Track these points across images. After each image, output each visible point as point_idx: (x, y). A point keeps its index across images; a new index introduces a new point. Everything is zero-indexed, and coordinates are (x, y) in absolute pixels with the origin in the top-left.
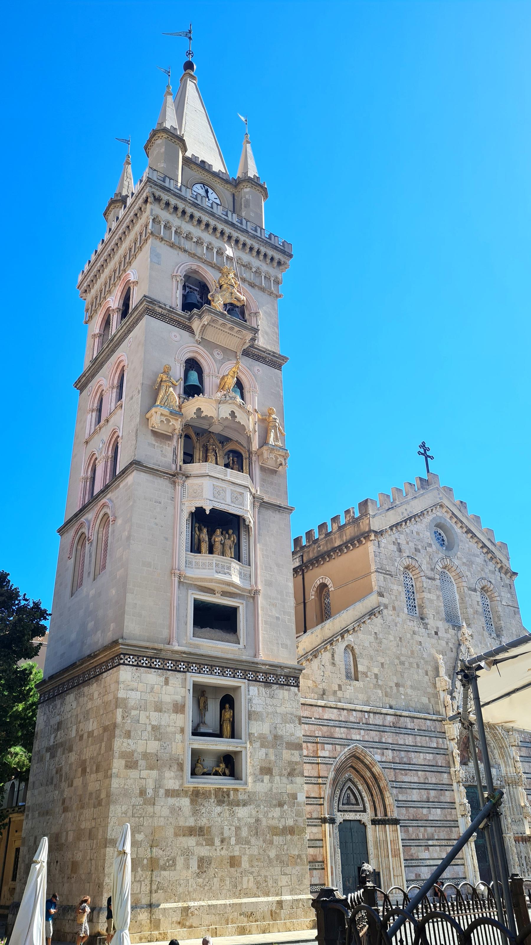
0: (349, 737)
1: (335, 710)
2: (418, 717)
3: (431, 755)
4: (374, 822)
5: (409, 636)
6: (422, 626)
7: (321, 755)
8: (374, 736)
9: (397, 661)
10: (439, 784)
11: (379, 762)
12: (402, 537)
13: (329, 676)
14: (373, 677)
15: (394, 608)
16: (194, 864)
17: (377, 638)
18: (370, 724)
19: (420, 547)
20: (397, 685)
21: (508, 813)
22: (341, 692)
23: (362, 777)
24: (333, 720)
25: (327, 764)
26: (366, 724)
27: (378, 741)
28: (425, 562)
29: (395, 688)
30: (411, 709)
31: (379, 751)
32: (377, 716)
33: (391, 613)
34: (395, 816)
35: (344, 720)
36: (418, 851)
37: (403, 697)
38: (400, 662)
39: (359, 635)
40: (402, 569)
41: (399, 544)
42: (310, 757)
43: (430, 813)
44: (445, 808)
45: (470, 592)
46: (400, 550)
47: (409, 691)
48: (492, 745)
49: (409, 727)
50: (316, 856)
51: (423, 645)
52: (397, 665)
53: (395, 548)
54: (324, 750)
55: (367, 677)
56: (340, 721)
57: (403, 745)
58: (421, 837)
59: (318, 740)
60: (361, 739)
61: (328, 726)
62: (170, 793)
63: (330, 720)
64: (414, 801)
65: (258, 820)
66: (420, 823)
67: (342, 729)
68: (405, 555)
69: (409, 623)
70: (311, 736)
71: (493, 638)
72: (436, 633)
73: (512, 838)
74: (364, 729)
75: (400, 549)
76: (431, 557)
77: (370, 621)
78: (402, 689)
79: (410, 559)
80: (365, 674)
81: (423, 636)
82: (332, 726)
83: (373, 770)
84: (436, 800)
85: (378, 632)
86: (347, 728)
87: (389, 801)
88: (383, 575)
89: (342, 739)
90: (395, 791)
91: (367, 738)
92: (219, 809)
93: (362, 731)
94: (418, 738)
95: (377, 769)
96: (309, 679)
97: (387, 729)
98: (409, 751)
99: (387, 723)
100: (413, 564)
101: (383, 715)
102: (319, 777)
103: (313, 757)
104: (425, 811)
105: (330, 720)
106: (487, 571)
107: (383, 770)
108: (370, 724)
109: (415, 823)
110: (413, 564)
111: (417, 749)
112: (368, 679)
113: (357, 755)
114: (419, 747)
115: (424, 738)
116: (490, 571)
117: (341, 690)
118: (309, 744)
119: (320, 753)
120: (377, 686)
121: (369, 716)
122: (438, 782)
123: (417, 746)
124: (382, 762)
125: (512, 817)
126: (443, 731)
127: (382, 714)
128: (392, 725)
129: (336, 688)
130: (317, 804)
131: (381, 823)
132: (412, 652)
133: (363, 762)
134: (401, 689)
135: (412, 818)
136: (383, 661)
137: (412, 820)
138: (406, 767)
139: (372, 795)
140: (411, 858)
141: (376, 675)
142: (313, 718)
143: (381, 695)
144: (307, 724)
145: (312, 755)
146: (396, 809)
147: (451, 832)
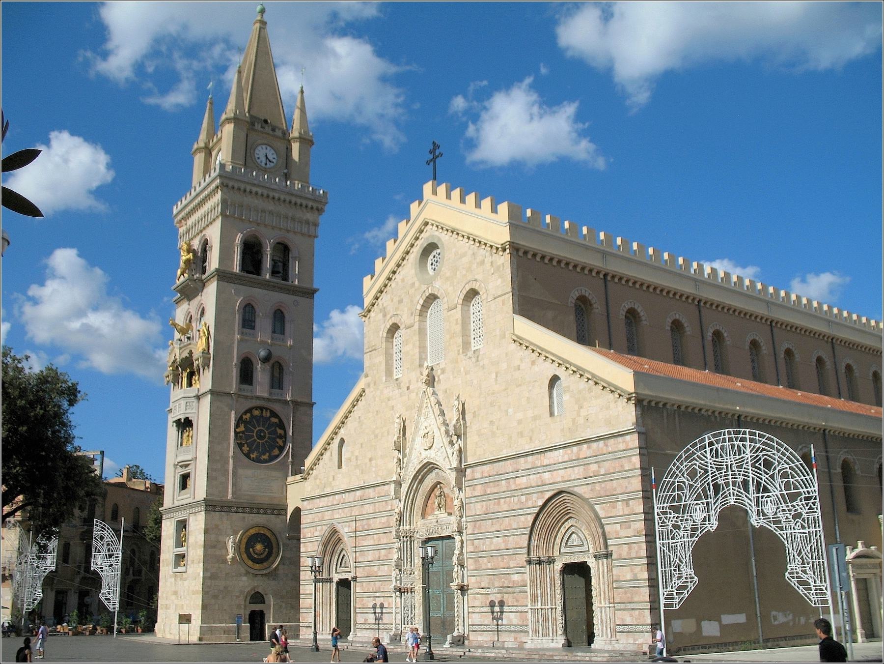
14: (355, 459)
15: (375, 384)
16: (174, 606)
28: (406, 309)
36: (368, 602)
43: (379, 569)
53: (381, 314)
58: (371, 590)
62: (171, 577)
65: (189, 587)
72: (408, 388)
84: (385, 558)
92: (180, 582)
104: (376, 568)
109: (368, 579)
111: (375, 515)
120: (357, 466)
134: (374, 462)
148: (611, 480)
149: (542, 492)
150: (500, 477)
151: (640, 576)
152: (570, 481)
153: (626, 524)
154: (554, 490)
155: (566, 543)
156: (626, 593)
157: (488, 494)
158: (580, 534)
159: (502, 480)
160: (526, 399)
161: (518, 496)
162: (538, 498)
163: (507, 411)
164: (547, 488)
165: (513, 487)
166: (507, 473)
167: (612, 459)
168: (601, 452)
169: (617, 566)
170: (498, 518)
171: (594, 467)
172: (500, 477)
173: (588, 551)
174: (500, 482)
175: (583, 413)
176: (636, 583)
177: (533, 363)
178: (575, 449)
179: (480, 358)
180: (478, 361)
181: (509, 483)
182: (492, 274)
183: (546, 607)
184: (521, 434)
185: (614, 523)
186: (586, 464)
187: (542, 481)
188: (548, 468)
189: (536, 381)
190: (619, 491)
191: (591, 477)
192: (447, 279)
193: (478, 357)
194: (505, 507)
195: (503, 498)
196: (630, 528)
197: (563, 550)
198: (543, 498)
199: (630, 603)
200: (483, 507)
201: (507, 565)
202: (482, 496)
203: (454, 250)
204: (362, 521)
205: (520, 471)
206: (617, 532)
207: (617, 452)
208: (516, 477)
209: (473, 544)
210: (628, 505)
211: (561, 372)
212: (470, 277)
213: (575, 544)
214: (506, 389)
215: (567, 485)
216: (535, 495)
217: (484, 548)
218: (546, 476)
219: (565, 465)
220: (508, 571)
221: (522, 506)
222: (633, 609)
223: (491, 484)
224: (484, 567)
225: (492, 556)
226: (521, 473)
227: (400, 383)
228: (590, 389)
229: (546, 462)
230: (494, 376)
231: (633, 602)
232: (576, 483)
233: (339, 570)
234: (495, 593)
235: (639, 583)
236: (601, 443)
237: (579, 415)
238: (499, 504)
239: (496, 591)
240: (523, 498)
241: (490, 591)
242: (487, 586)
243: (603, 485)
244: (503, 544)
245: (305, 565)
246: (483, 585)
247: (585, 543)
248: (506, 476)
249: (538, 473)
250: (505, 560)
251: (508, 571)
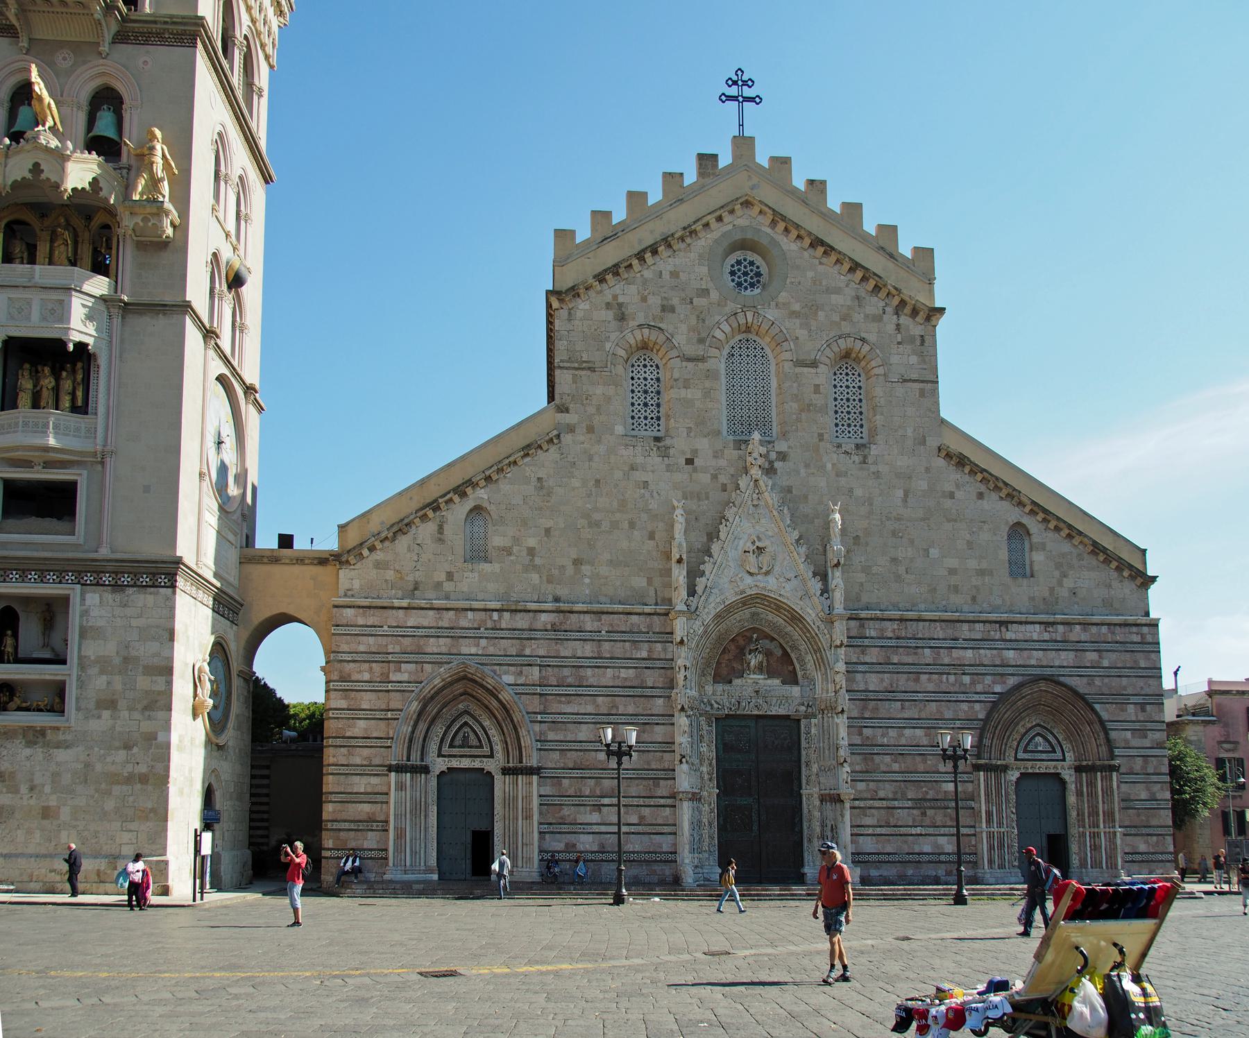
0: (455, 651)
1: (431, 613)
2: (610, 610)
3: (631, 671)
4: (506, 771)
5: (618, 474)
6: (654, 453)
7: (394, 679)
8: (511, 647)
9: (582, 522)
10: (642, 715)
11: (509, 685)
12: (633, 289)
13: (429, 560)
14: (524, 553)
15: (590, 429)
17: (542, 488)
18: (502, 630)
19: (675, 301)
20: (577, 562)
21: (813, 756)
22: (451, 583)
23: (487, 707)
24: (425, 628)
25: (404, 691)
26: (492, 629)
27: (515, 654)
28: (683, 328)
29: (570, 570)
30: (602, 599)
31: (512, 669)
32: (519, 615)
33: (582, 438)
34: (534, 762)
35: (447, 625)
37: (587, 581)
38: (590, 525)
39: (502, 486)
40: (622, 353)
41: (620, 305)
42: (376, 682)
44: (648, 751)
45: (798, 370)
46: (622, 318)
47: (604, 570)
48: (802, 648)
49: (589, 629)
50: (374, 814)
51: (651, 487)
52: (583, 527)
53: (609, 315)
54: (400, 671)
55: (510, 554)
56: (438, 628)
57: (571, 658)
58: (587, 793)
59: (390, 657)
60: (480, 653)
61: (414, 636)
63: (418, 628)
64: (581, 742)
66: (587, 773)
67: (440, 639)
68: (632, 324)
69: (622, 451)
70: (379, 653)
71: (846, 453)
72: (690, 462)
73: (816, 796)
74: (486, 638)
75: (623, 314)
76: (701, 316)
77: (527, 459)
78: (588, 567)
79: (646, 331)
80: (508, 551)
81: (653, 472)
82: (422, 636)
83: (500, 696)
85: (544, 476)
86: (452, 637)
87: (526, 741)
88: (571, 372)
89: (440, 654)
90: (537, 727)
91: (491, 650)
93: (483, 642)
94: (606, 646)
95: (505, 696)
96: (388, 569)
97: (538, 634)
98: (581, 667)
99: (539, 625)
100: (653, 338)
101: (531, 614)
102: (389, 710)
103: (380, 682)
105: (418, 628)
106: (858, 317)
107: (516, 697)
108: (502, 630)
109: (576, 773)
110: (653, 338)
111: (600, 662)
112: (512, 558)
113: (470, 676)
114: (607, 658)
115: (619, 645)
116: (867, 316)
117: (452, 580)
118: (374, 665)
119: (393, 677)
120: (531, 567)
121: (500, 618)
122: (640, 711)
123: (601, 658)
124: (518, 685)
125: (821, 763)
126: (668, 630)
127: (529, 611)
128: (549, 627)
129: (443, 577)
130: (381, 747)
131: (524, 772)
132: (623, 503)
133: (482, 686)
134: (586, 569)
135: (571, 766)
136: (550, 524)
137: (570, 769)
138: (571, 691)
139: (504, 734)
140: (561, 821)
141: (531, 552)
142: (386, 628)
143: (537, 582)
144: (372, 635)
145: (378, 680)
146: (535, 754)
147: (658, 786)
148: (1119, 676)
149: (1002, 675)
150: (920, 643)
151: (1159, 796)
152: (1052, 667)
153: (1142, 733)
154: (1022, 675)
155: (1028, 744)
156: (1139, 815)
157: (895, 664)
158: (1050, 738)
159: (923, 647)
160: (965, 542)
161: (955, 674)
162: (994, 683)
163: (927, 551)
164: (1010, 670)
165: (946, 661)
166: (934, 639)
167: (1121, 651)
168: (1103, 639)
169: (1126, 782)
170: (915, 700)
171: (1092, 656)
172: (920, 643)
173: (1064, 760)
174: (920, 650)
175: (1068, 583)
176: (1154, 804)
177: (980, 496)
178: (1061, 628)
179: (870, 460)
180: (864, 462)
181: (938, 654)
182: (899, 343)
183: (1002, 830)
184: (956, 589)
185: (1123, 730)
186: (1080, 650)
187: (1002, 660)
188: (1014, 645)
189: (984, 522)
190: (1130, 691)
191: (1088, 667)
192: (794, 314)
193: (865, 457)
194: (931, 687)
195: (926, 673)
196: (1146, 738)
197: (1021, 755)
198: (1005, 683)
199: (1145, 827)
200: (882, 680)
201: (934, 769)
202: (880, 664)
203: (810, 274)
204: (556, 670)
205: (961, 641)
206: (1126, 741)
207: (1127, 643)
208: (953, 648)
209: (860, 734)
210: (1143, 710)
211: (1032, 524)
212: (846, 328)
213: (1040, 748)
214: (923, 519)
215: (1048, 671)
216: (989, 678)
217: (885, 741)
218: (1011, 654)
219: (1044, 646)
220: (936, 777)
221: (963, 689)
222: (1148, 835)
223: (901, 650)
224: (883, 768)
225: (903, 754)
226: (960, 643)
227: (667, 448)
228: (1079, 555)
229: (1009, 635)
230: (900, 493)
231: (1150, 827)
232: (1062, 671)
233: (446, 750)
234: (908, 808)
235: (1159, 804)
236: (1104, 629)
237: (1060, 584)
238: (917, 680)
239: (910, 804)
240: (967, 679)
241: (896, 803)
242: (891, 796)
243: (1106, 680)
244: (924, 738)
245: (348, 734)
246: (881, 794)
247: (1058, 749)
248: (932, 643)
249: (995, 649)
250: (929, 762)
251: (936, 777)
